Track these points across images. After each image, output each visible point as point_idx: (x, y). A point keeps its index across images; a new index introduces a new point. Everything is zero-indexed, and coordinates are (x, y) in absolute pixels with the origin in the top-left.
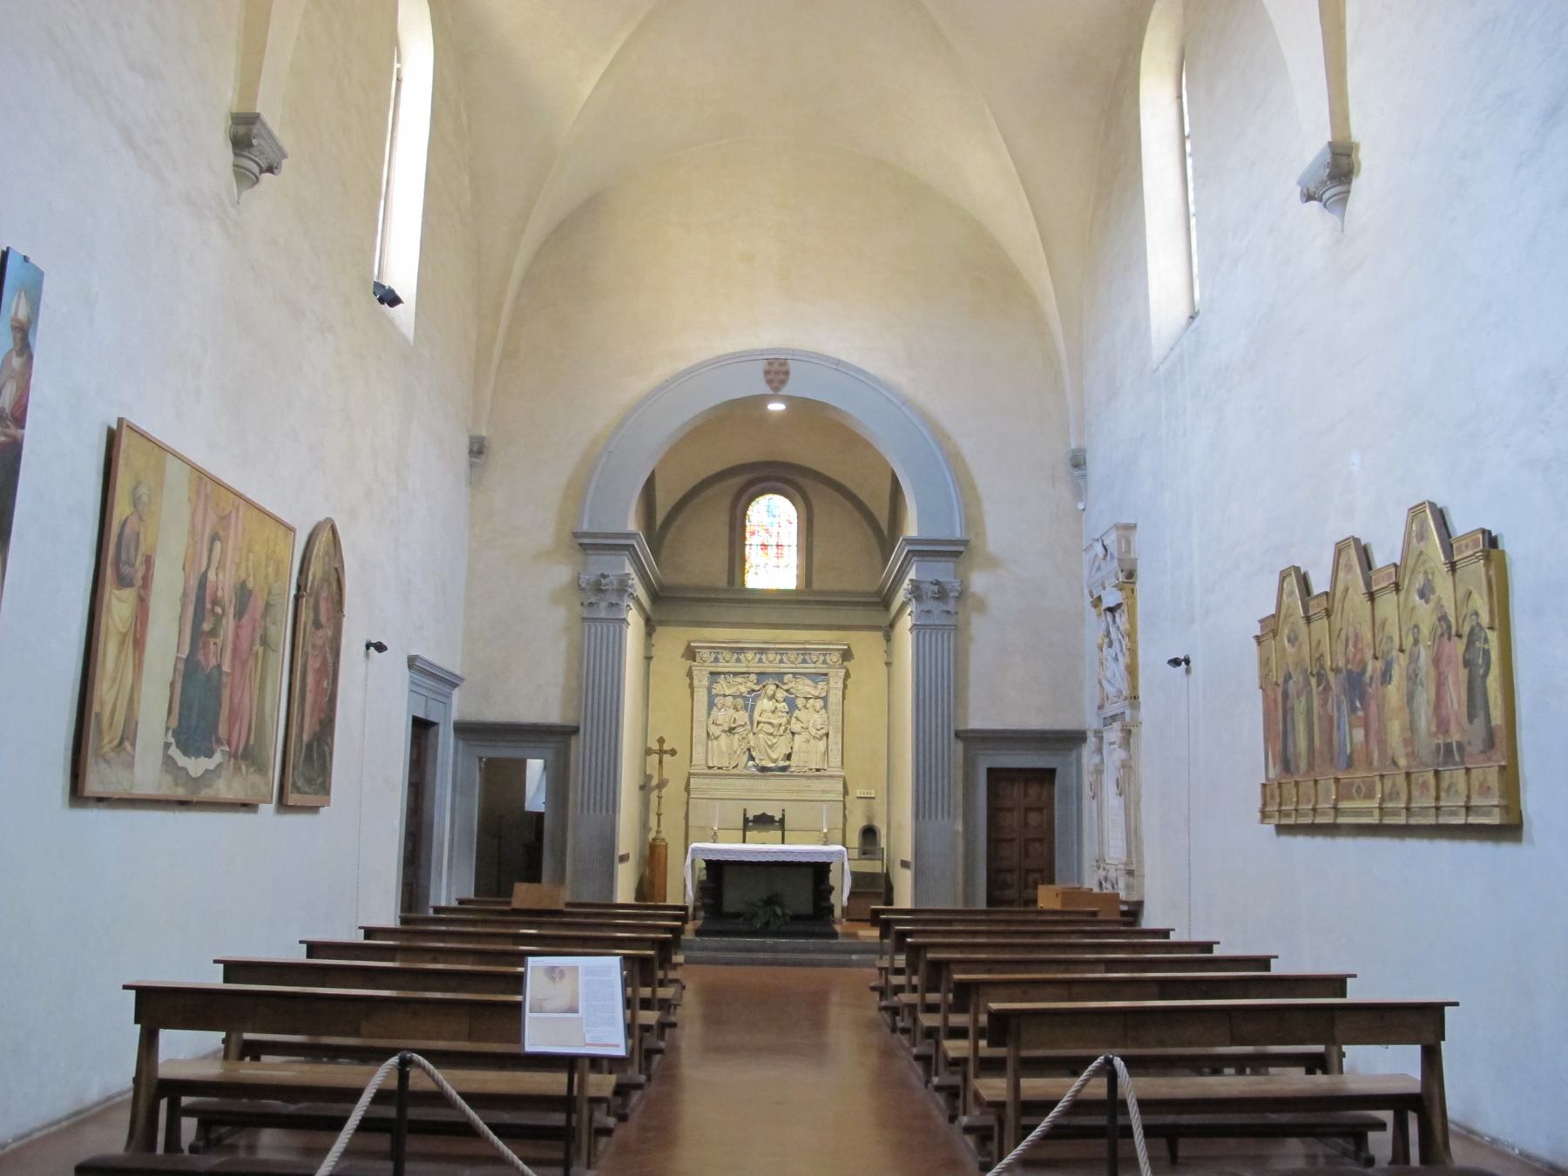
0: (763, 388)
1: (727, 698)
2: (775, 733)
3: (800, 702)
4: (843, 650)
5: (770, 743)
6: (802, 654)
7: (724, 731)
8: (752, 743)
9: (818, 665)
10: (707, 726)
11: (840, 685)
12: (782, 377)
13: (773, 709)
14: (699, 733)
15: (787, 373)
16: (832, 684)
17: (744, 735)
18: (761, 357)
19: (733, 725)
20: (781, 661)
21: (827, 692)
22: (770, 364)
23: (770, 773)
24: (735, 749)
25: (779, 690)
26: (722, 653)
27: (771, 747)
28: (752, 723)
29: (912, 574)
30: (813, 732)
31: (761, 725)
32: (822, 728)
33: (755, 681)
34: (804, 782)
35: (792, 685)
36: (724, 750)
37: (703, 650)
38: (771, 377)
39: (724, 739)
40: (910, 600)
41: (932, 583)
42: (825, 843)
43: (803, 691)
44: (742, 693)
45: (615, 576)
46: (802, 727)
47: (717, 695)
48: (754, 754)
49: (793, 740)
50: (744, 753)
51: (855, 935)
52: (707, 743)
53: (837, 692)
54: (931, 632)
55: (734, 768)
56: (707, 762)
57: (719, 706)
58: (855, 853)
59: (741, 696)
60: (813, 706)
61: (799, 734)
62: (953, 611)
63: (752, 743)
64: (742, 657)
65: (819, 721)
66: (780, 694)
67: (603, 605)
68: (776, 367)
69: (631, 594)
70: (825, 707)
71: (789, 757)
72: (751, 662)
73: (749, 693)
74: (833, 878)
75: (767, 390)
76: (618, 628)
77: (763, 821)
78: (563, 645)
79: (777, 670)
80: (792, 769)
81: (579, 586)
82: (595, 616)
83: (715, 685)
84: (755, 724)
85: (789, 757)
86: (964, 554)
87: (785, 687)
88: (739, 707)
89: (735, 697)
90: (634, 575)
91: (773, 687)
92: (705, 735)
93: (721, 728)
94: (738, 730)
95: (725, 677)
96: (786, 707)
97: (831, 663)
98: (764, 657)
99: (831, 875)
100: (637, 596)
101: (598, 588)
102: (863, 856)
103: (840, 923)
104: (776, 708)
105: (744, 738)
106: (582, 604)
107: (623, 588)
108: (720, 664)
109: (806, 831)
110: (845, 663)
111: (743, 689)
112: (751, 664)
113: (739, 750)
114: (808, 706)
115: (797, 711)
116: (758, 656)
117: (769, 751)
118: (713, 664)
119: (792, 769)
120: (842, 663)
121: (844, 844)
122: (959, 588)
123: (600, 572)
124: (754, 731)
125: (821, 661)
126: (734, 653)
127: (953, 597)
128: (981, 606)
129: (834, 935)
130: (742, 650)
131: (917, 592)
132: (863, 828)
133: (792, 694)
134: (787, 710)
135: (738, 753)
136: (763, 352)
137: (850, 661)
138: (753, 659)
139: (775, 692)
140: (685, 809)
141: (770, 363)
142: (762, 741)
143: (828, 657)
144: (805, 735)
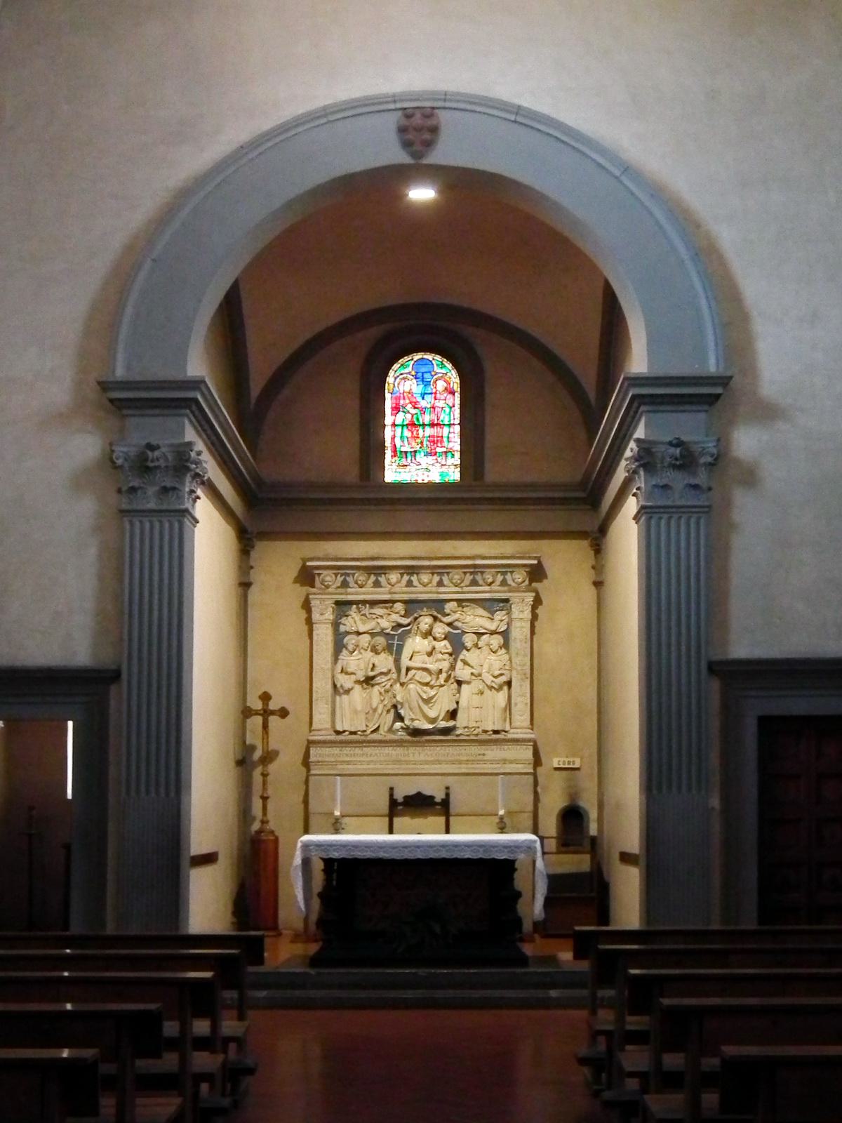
0: (396, 155)
1: (361, 636)
2: (432, 683)
3: (469, 640)
5: (425, 697)
7: (358, 682)
8: (399, 698)
10: (333, 677)
12: (427, 136)
13: (429, 649)
14: (322, 686)
15: (434, 130)
17: (388, 687)
18: (392, 106)
19: (372, 674)
20: (440, 584)
22: (408, 117)
23: (428, 738)
24: (374, 706)
25: (438, 624)
26: (354, 574)
27: (428, 701)
28: (399, 670)
29: (640, 433)
30: (488, 679)
31: (411, 673)
32: (501, 675)
33: (403, 613)
34: (475, 750)
35: (457, 616)
36: (359, 708)
38: (410, 136)
39: (358, 693)
40: (635, 472)
41: (671, 444)
42: (502, 830)
44: (383, 630)
45: (172, 445)
46: (472, 674)
47: (348, 633)
48: (402, 712)
49: (459, 692)
50: (388, 711)
51: (553, 960)
52: (334, 702)
54: (670, 518)
55: (372, 732)
56: (333, 722)
57: (351, 647)
58: (552, 845)
59: (382, 633)
60: (488, 645)
61: (468, 683)
62: (705, 486)
63: (399, 698)
64: (382, 579)
65: (497, 665)
66: (440, 629)
67: (152, 490)
68: (417, 120)
69: (197, 475)
70: (506, 645)
71: (453, 715)
72: (395, 587)
73: (393, 628)
74: (520, 881)
75: (403, 158)
76: (176, 525)
77: (419, 804)
78: (92, 552)
79: (434, 596)
80: (458, 732)
81: (113, 462)
82: (140, 507)
84: (404, 671)
85: (453, 715)
86: (722, 398)
88: (379, 648)
89: (373, 635)
90: (200, 445)
91: (429, 620)
92: (329, 686)
93: (353, 678)
94: (378, 680)
95: (358, 608)
96: (448, 646)
98: (414, 578)
99: (516, 875)
100: (209, 479)
101: (143, 465)
102: (564, 849)
103: (532, 940)
104: (434, 648)
105: (387, 691)
106: (119, 491)
107: (182, 463)
109: (478, 815)
111: (385, 624)
112: (396, 589)
113: (381, 707)
114: (480, 644)
115: (465, 652)
116: (406, 578)
117: (425, 708)
119: (458, 732)
121: (535, 831)
122: (715, 451)
123: (144, 443)
124: (403, 680)
126: (369, 574)
127: (705, 464)
128: (749, 477)
129: (523, 961)
130: (383, 570)
131: (646, 459)
132: (558, 815)
133: (457, 628)
134: (450, 650)
135: (379, 711)
136: (394, 99)
138: (399, 582)
139: (431, 627)
140: (303, 793)
141: (408, 117)
142: (413, 694)
144: (477, 685)
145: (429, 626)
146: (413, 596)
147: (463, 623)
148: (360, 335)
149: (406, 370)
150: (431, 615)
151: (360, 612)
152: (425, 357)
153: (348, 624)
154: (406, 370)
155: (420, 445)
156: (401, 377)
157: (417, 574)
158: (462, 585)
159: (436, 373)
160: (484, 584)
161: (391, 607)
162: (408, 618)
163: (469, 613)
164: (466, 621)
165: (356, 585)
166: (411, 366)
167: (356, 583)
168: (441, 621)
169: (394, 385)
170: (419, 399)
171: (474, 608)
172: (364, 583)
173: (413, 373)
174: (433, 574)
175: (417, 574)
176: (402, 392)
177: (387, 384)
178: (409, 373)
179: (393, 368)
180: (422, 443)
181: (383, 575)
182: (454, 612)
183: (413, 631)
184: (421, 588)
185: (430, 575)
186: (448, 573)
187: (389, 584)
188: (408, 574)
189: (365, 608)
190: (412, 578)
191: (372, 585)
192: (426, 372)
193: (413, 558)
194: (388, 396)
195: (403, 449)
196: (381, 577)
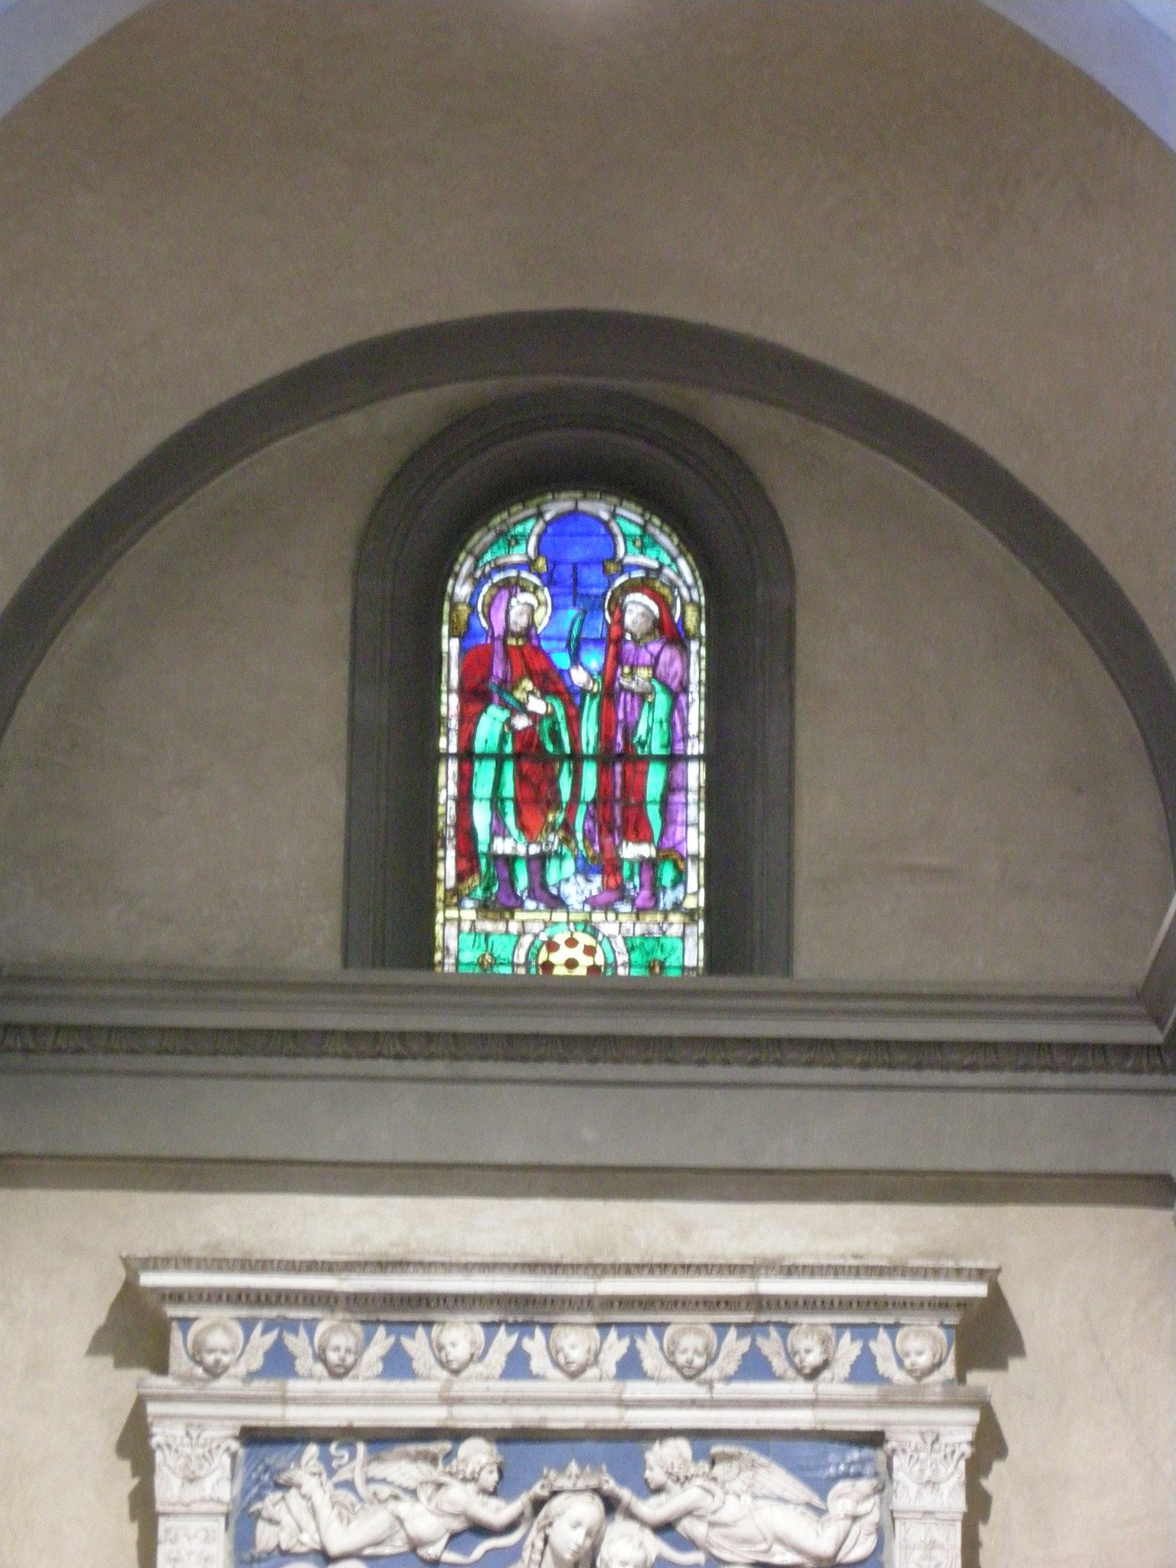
4: (963, 1304)
6: (744, 1328)
9: (831, 1385)
11: (952, 1498)
16: (907, 1491)
20: (630, 1367)
21: (882, 1535)
26: (311, 1326)
33: (490, 1479)
37: (208, 1315)
43: (744, 1530)
44: (414, 1545)
53: (938, 1533)
64: (417, 1345)
79: (607, 1417)
83: (271, 1503)
87: (654, 1509)
91: (589, 1509)
95: (326, 1459)
97: (899, 1376)
98: (535, 1344)
108: (295, 1387)
110: (976, 1378)
112: (462, 1386)
116: (504, 1341)
118: (260, 1386)
120: (961, 1378)
125: (842, 1366)
126: (370, 1325)
133: (688, 1544)
137: (997, 1362)
138: (478, 1357)
143: (881, 1345)
145: (588, 1534)
146: (528, 1416)
147: (712, 1525)
148: (353, 423)
149: (517, 555)
150: (597, 1491)
151: (332, 1473)
152: (585, 506)
153: (286, 1519)
154: (517, 555)
155: (561, 834)
156: (497, 578)
157: (548, 1327)
158: (712, 1372)
159: (624, 568)
160: (791, 1373)
161: (449, 1456)
162: (510, 1497)
163: (737, 1485)
164: (722, 1516)
165: (319, 1368)
166: (533, 540)
167: (321, 1357)
168: (630, 1515)
169: (472, 606)
170: (561, 660)
171: (753, 1465)
172: (350, 1359)
173: (541, 563)
174: (604, 1327)
175: (548, 1327)
176: (499, 630)
177: (446, 607)
178: (529, 565)
179: (470, 545)
180: (568, 827)
181: (420, 1331)
182: (683, 1481)
183: (526, 1554)
184: (557, 1384)
185: (595, 1333)
186: (660, 1327)
187: (444, 1364)
188: (511, 1326)
189: (353, 1457)
190: (528, 1344)
191: (380, 1367)
192: (587, 563)
193: (533, 1267)
194: (451, 646)
195: (502, 846)
196: (413, 1336)
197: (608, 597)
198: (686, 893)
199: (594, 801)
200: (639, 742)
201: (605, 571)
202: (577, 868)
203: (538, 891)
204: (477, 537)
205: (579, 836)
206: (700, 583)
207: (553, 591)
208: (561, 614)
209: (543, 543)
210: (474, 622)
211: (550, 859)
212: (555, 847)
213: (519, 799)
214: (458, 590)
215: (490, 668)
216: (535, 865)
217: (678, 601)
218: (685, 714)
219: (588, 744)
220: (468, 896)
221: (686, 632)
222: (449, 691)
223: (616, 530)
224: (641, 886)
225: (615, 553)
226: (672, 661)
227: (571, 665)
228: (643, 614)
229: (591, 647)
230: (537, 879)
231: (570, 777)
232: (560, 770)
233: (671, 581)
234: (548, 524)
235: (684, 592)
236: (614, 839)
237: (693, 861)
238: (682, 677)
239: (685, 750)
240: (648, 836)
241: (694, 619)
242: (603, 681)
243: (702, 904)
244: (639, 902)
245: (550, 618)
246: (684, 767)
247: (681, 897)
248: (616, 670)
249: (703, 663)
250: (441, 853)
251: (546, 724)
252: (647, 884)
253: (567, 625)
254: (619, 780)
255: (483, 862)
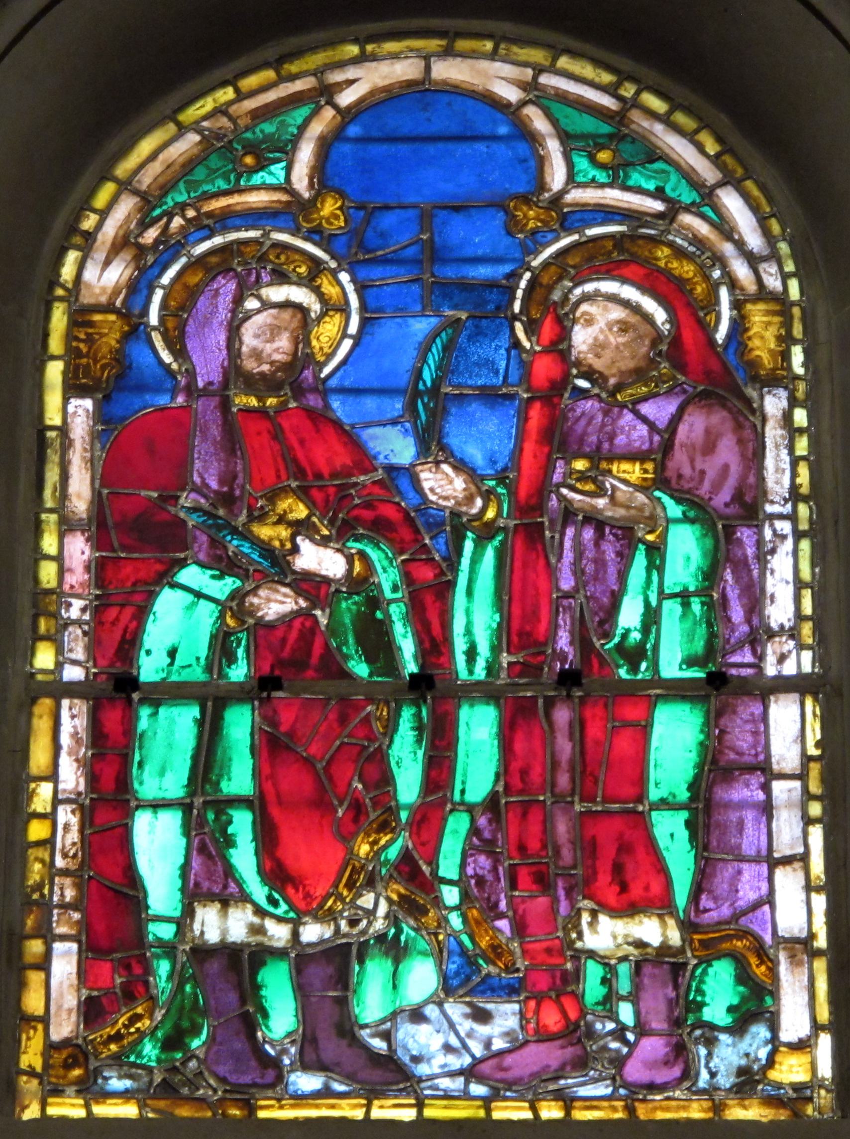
166: (306, 154)
177: (59, 319)
179: (124, 168)
197: (523, 284)
198: (774, 1040)
199: (492, 803)
200: (620, 647)
201: (512, 226)
202: (445, 978)
203: (331, 1047)
204: (146, 146)
205: (451, 895)
206: (784, 247)
207: (363, 273)
208: (386, 331)
209: (334, 156)
210: (139, 355)
211: (361, 961)
212: (379, 925)
213: (271, 797)
214: (90, 274)
215: (183, 464)
216: (318, 973)
217: (724, 294)
218: (755, 573)
219: (471, 654)
220: (117, 1060)
221: (753, 365)
222: (67, 526)
223: (540, 123)
224: (642, 1029)
225: (542, 186)
226: (709, 447)
227: (418, 455)
228: (624, 327)
229: (476, 408)
230: (327, 1015)
231: (419, 741)
232: (391, 727)
233: (697, 241)
234: (348, 115)
235: (741, 270)
236: (556, 900)
237: (792, 957)
238: (743, 478)
239: (758, 666)
240: (656, 888)
241: (770, 335)
242: (513, 493)
243: (825, 1069)
244: (634, 1071)
245: (358, 340)
246: (756, 709)
247: (763, 1053)
248: (548, 468)
249: (802, 446)
250: (35, 947)
251: (348, 607)
252: (658, 1023)
253: (407, 360)
254: (565, 747)
255: (163, 967)
